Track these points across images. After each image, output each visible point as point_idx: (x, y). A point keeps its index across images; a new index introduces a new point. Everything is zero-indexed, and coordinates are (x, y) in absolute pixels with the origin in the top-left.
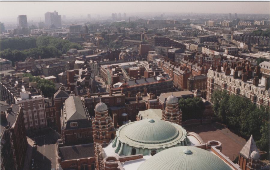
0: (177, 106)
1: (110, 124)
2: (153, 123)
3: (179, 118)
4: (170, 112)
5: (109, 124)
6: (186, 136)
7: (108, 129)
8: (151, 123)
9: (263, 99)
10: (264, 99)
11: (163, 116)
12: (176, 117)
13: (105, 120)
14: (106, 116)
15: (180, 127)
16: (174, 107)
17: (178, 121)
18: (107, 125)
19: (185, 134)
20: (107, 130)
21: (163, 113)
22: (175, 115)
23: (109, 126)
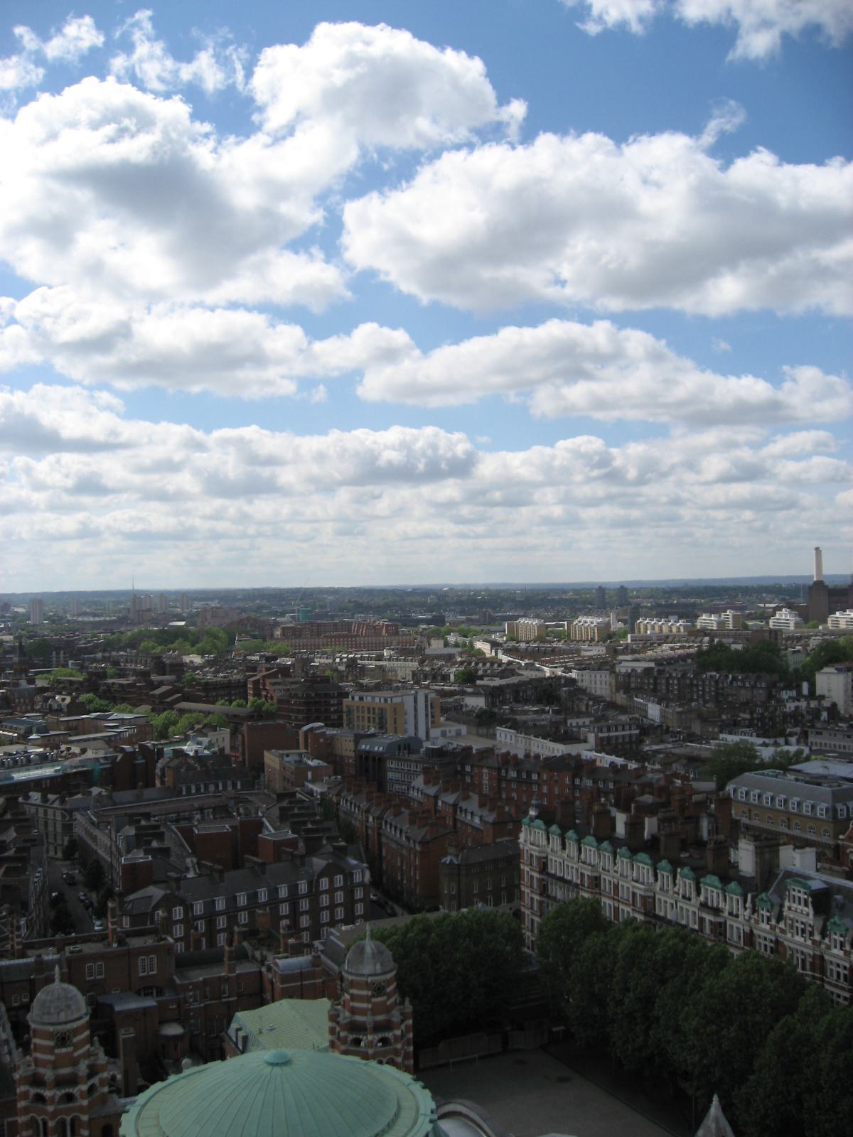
0: (389, 983)
1: (95, 1080)
2: (286, 1069)
3: (403, 1035)
4: (363, 1012)
5: (90, 1083)
6: (431, 1121)
7: (85, 1103)
8: (277, 1070)
9: (751, 931)
10: (755, 931)
11: (332, 1031)
12: (389, 1035)
13: (75, 1062)
14: (77, 1047)
15: (407, 1078)
16: (379, 990)
17: (396, 1052)
18: (84, 1088)
19: (429, 1112)
20: (82, 1109)
21: (334, 1017)
22: (387, 1026)
23: (92, 1089)
